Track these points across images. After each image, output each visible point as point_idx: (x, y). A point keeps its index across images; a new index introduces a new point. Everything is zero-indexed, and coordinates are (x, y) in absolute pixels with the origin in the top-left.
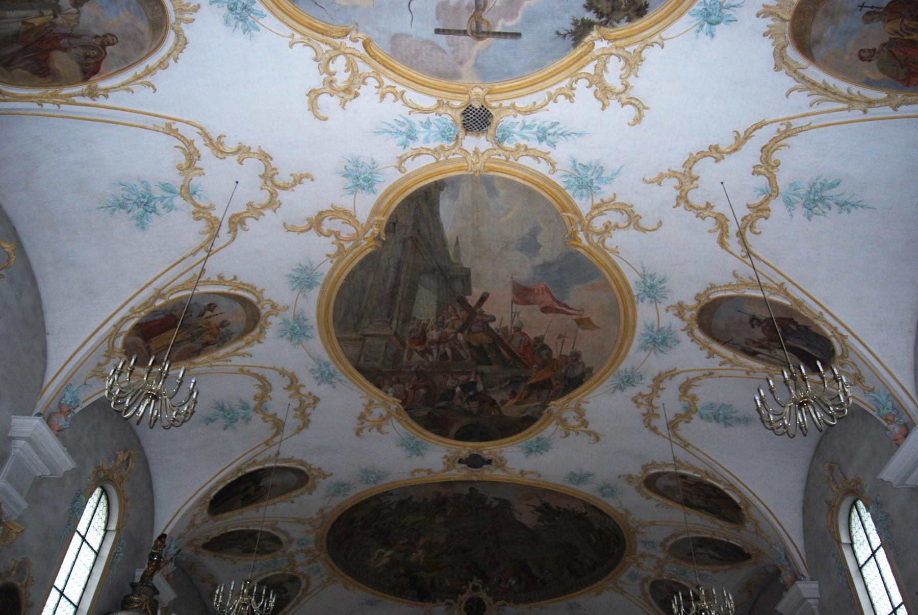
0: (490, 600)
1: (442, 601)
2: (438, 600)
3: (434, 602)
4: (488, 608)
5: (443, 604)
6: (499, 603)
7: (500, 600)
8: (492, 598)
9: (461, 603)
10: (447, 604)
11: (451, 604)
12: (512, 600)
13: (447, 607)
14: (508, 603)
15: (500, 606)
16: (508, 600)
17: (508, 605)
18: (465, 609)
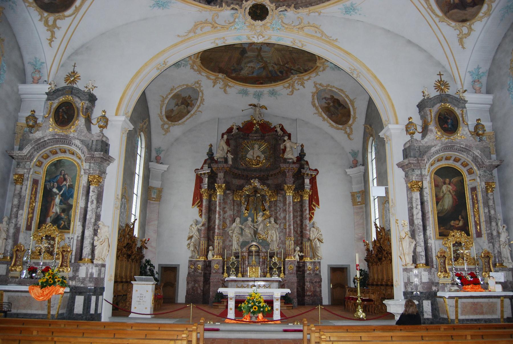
0: (273, 6)
1: (229, 6)
2: (224, 4)
3: (221, 6)
4: (270, 13)
5: (229, 8)
6: (280, 9)
7: (281, 6)
8: (274, 4)
9: (246, 8)
10: (233, 9)
11: (236, 9)
12: (293, 5)
13: (233, 11)
14: (289, 8)
15: (281, 11)
16: (289, 6)
17: (289, 10)
18: (250, 14)
